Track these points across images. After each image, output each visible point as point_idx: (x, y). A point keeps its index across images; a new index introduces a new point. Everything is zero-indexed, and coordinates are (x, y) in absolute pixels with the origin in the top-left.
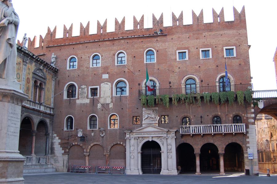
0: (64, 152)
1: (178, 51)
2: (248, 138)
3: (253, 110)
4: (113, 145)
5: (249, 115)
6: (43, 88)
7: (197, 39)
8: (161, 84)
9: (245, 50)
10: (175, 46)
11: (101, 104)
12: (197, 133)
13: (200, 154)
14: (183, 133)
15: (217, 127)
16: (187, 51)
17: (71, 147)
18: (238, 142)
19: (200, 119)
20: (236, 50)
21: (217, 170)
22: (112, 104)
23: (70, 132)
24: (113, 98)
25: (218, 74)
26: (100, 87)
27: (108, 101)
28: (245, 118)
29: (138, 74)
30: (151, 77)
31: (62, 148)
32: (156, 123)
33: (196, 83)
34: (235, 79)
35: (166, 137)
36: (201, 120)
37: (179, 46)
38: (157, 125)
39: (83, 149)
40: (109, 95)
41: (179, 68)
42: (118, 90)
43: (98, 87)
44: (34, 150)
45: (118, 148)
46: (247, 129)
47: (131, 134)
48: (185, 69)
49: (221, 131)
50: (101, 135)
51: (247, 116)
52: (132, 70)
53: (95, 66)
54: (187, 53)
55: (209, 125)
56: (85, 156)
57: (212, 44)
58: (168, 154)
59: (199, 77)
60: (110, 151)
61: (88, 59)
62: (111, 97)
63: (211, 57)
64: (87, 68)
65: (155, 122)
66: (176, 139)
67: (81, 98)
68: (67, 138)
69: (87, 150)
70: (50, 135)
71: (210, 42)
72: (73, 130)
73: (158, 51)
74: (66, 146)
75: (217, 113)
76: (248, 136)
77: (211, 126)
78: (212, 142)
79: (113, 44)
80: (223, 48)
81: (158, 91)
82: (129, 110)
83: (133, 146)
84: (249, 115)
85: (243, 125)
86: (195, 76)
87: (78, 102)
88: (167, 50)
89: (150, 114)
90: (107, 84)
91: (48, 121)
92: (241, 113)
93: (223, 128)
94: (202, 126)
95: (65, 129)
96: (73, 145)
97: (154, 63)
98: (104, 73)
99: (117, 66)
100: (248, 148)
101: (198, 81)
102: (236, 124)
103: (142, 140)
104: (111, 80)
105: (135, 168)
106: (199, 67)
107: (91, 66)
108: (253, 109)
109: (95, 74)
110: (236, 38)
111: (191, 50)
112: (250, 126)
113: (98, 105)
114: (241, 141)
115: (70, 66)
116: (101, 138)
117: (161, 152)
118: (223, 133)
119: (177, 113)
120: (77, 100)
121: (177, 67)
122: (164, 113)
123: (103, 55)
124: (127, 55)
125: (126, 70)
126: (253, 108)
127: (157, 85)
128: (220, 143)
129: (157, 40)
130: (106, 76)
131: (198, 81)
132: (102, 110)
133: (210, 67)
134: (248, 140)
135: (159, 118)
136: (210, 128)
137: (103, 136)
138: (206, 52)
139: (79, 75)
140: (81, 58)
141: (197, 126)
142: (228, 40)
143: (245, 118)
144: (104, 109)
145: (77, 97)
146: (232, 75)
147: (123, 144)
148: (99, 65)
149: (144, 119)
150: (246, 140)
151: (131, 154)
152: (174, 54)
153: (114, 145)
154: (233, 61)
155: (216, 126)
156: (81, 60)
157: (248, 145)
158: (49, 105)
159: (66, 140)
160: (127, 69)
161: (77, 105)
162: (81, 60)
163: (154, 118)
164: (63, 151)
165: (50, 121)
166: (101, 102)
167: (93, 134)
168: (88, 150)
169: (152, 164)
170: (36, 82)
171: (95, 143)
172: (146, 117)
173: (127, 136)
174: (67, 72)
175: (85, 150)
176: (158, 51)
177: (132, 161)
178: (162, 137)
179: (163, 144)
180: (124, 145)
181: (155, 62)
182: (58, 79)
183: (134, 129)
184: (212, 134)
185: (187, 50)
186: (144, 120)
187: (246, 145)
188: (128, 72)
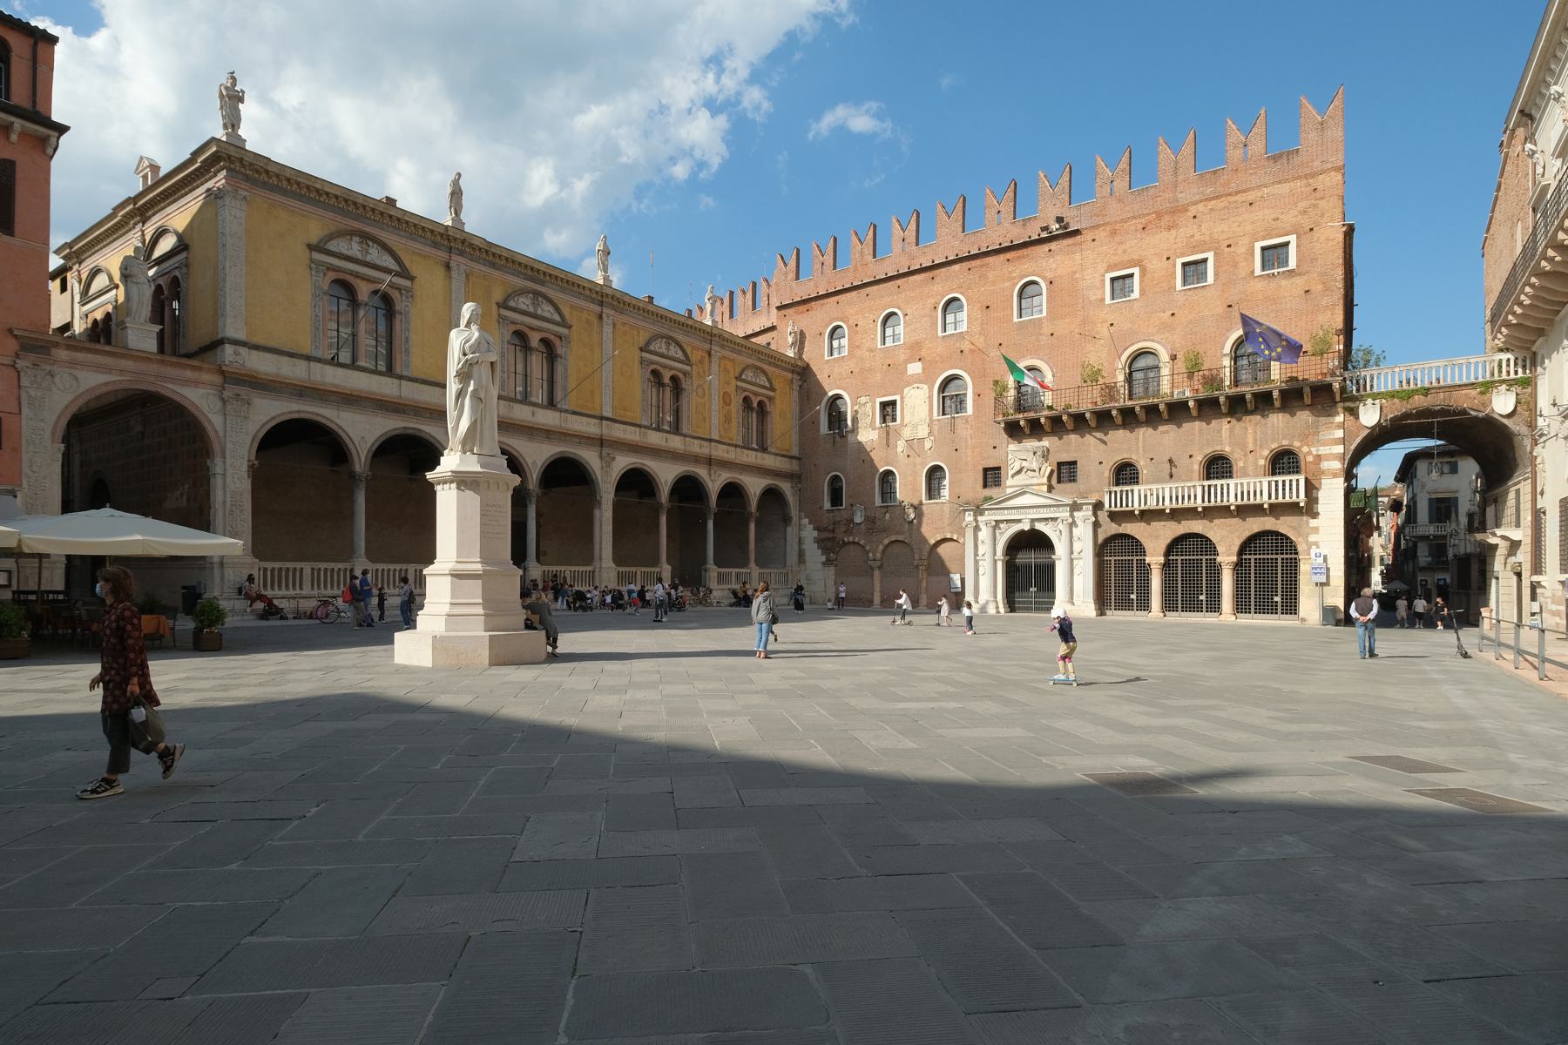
1: (1109, 276)
3: (1339, 434)
21: (1214, 606)
25: (1230, 330)
28: (1310, 459)
37: (1114, 260)
38: (1045, 488)
43: (897, 398)
54: (1136, 278)
64: (871, 351)
70: (795, 519)
74: (830, 544)
91: (786, 487)
92: (1297, 444)
93: (1232, 491)
94: (1167, 487)
95: (827, 505)
101: (1164, 356)
104: (926, 378)
110: (1303, 205)
125: (966, 346)
126: (1342, 426)
130: (915, 368)
131: (1164, 356)
141: (1154, 487)
143: (1310, 459)
154: (1284, 283)
168: (879, 555)
170: (746, 399)
171: (893, 538)
172: (1017, 468)
181: (1045, 313)
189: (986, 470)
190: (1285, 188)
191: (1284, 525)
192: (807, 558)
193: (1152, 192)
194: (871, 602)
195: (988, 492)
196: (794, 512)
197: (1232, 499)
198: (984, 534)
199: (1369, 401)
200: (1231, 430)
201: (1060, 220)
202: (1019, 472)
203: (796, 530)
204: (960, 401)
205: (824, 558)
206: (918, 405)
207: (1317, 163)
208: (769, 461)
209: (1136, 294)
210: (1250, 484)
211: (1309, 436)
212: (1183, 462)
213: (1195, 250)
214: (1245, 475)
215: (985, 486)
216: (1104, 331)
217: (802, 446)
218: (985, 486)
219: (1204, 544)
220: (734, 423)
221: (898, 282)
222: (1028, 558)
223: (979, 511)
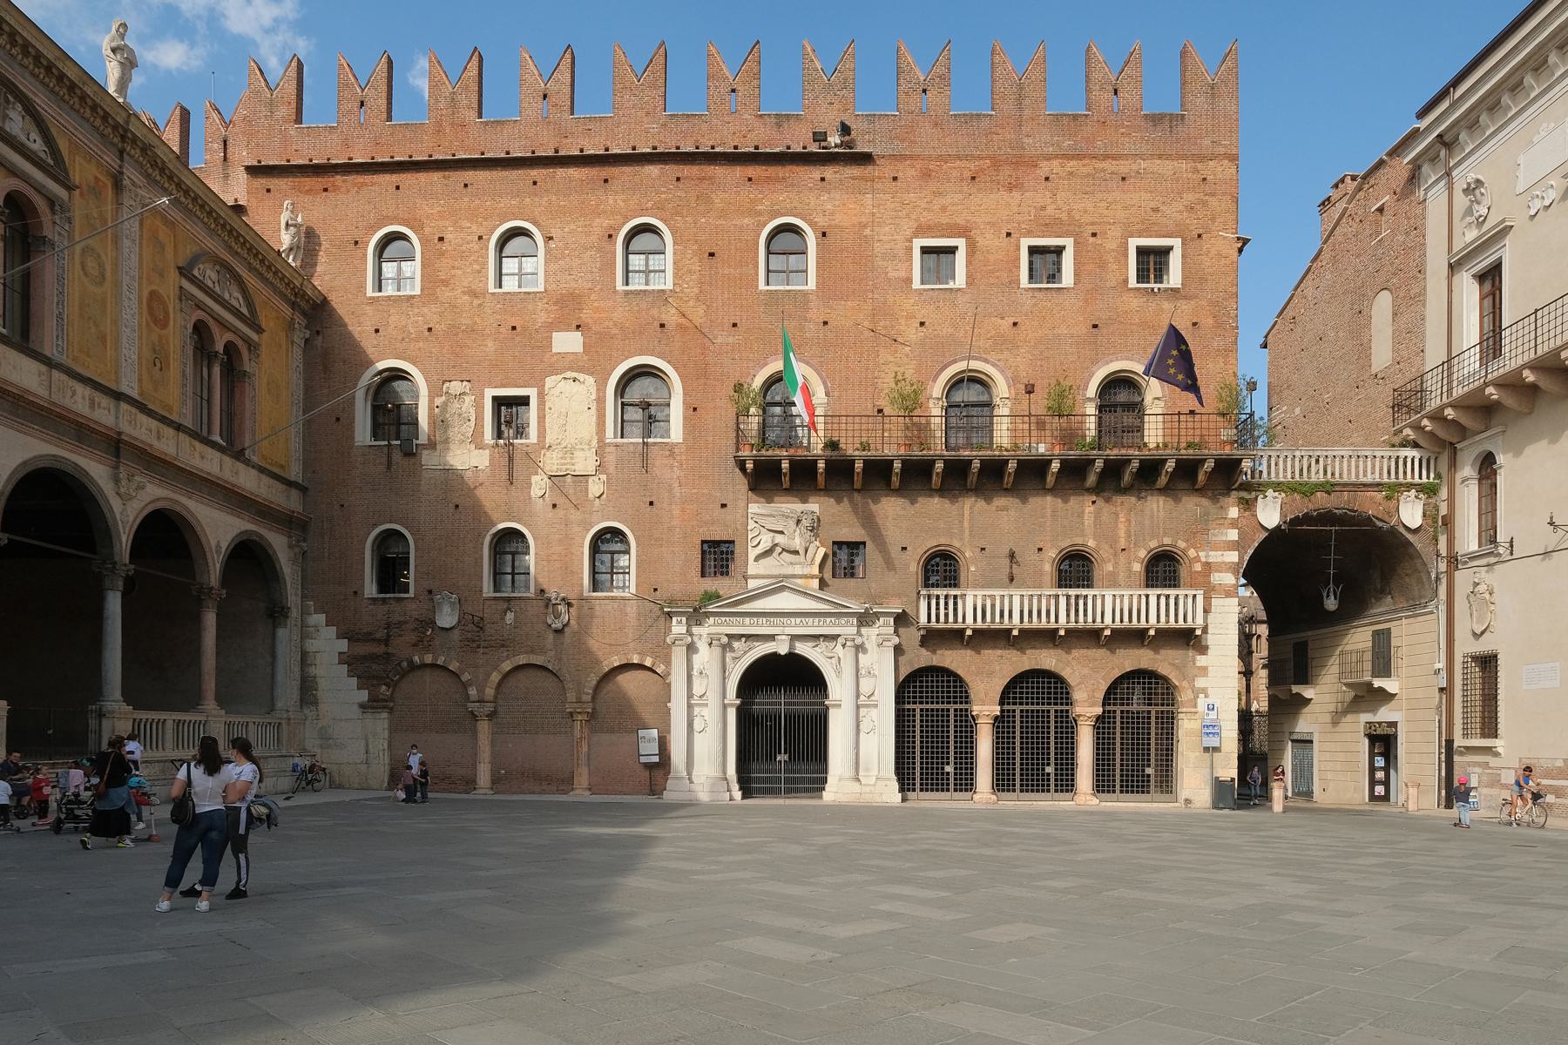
1: (919, 243)
2: (1203, 650)
3: (1233, 535)
5: (1215, 557)
11: (550, 477)
13: (996, 718)
17: (404, 674)
18: (1163, 669)
19: (1007, 561)
22: (603, 477)
25: (1095, 362)
27: (585, 462)
28: (1198, 567)
29: (730, 339)
32: (812, 577)
33: (997, 401)
37: (926, 217)
38: (816, 582)
39: (465, 686)
41: (922, 324)
42: (634, 414)
43: (532, 392)
44: (210, 685)
48: (947, 331)
54: (961, 257)
56: (474, 716)
60: (594, 698)
62: (594, 443)
64: (473, 294)
65: (807, 571)
68: (381, 634)
69: (481, 691)
70: (295, 613)
71: (1069, 212)
73: (824, 234)
74: (380, 668)
75: (1079, 541)
82: (683, 510)
86: (994, 365)
88: (867, 232)
92: (1181, 544)
95: (370, 589)
96: (413, 667)
97: (805, 294)
99: (627, 293)
101: (1002, 389)
102: (1166, 591)
104: (591, 363)
106: (1015, 324)
107: (492, 289)
109: (514, 328)
110: (1189, 197)
111: (981, 241)
113: (535, 479)
116: (551, 636)
120: (425, 452)
121: (910, 317)
125: (671, 317)
128: (1086, 671)
129: (823, 179)
130: (568, 342)
132: (554, 506)
133: (1063, 330)
135: (822, 551)
137: (558, 625)
139: (430, 330)
142: (1152, 204)
144: (560, 501)
150: (1194, 661)
152: (901, 253)
156: (442, 254)
157: (1200, 683)
162: (442, 254)
163: (802, 552)
166: (547, 469)
168: (490, 692)
171: (522, 659)
175: (473, 692)
176: (824, 234)
178: (834, 637)
179: (839, 673)
181: (812, 284)
182: (319, 341)
186: (757, 559)
190: (1166, 167)
191: (1163, 662)
193: (985, 123)
194: (470, 783)
196: (293, 598)
198: (705, 657)
199: (1270, 492)
200: (1097, 515)
201: (845, 130)
202: (768, 553)
203: (296, 637)
204: (651, 417)
205: (364, 696)
206: (572, 416)
207: (1207, 142)
209: (960, 280)
210: (1115, 601)
211: (1199, 533)
212: (1027, 556)
213: (1050, 227)
214: (1114, 584)
216: (912, 334)
219: (1051, 686)
221: (535, 173)
222: (779, 703)
223: (697, 616)
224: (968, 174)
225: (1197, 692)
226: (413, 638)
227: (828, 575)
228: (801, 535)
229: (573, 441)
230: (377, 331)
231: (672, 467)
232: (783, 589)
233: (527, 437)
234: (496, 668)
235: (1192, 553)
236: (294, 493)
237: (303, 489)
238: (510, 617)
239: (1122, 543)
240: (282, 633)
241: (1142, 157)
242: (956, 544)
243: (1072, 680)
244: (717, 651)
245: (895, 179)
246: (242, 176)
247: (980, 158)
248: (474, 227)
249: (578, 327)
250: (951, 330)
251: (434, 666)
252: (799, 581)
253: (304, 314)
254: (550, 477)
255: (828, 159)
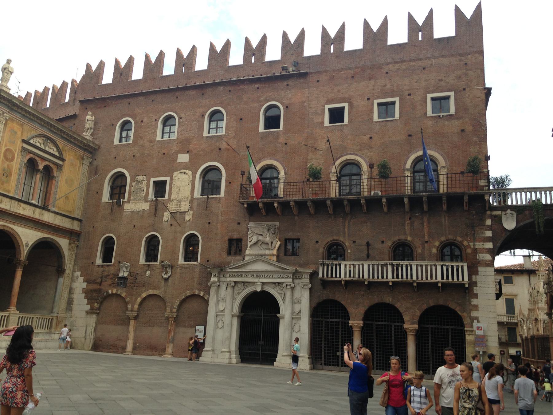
0: (90, 309)
1: (327, 107)
2: (477, 298)
3: (489, 234)
4: (184, 297)
5: (479, 245)
6: (53, 177)
7: (370, 79)
8: (289, 173)
9: (477, 100)
10: (323, 96)
11: (171, 213)
12: (354, 279)
14: (325, 278)
15: (400, 268)
16: (346, 105)
18: (452, 305)
19: (366, 247)
20: (456, 100)
22: (191, 212)
23: (106, 269)
24: (195, 201)
25: (410, 152)
26: (171, 180)
27: (185, 206)
30: (271, 159)
31: (88, 299)
33: (362, 172)
34: (448, 162)
35: (290, 285)
36: (368, 250)
38: (275, 258)
39: (127, 304)
40: (187, 196)
42: (206, 184)
43: (168, 179)
45: (194, 305)
46: (474, 277)
47: (222, 276)
49: (409, 277)
50: (163, 275)
51: (474, 245)
52: (234, 147)
53: (166, 137)
55: (382, 263)
57: (401, 88)
58: (294, 321)
59: (367, 160)
61: (153, 123)
62: (189, 198)
63: (397, 116)
64: (151, 141)
65: (271, 252)
66: (310, 289)
67: (135, 199)
68: (99, 280)
69: (133, 306)
70: (67, 271)
72: (112, 263)
73: (287, 107)
75: (403, 237)
76: (475, 292)
77: (386, 265)
78: (388, 299)
79: (203, 94)
80: (426, 97)
81: (282, 187)
83: (224, 300)
84: (479, 245)
85: (462, 267)
87: (128, 207)
88: (305, 104)
89: (261, 235)
90: (185, 173)
91: (63, 243)
92: (459, 239)
93: (416, 271)
98: (182, 152)
99: (207, 137)
100: (475, 321)
101: (365, 167)
103: (243, 288)
104: (192, 166)
105: (223, 350)
106: (371, 138)
107: (159, 138)
108: (488, 230)
109: (164, 154)
110: (458, 73)
111: (355, 103)
112: (481, 269)
113: (165, 213)
114: (458, 303)
115: (121, 138)
116: (163, 282)
117: (278, 315)
118: (414, 281)
119: (315, 236)
122: (290, 233)
123: (183, 116)
124: (227, 116)
125: (223, 145)
127: (280, 177)
130: (183, 158)
131: (365, 167)
132: (171, 225)
134: (474, 302)
135: (279, 243)
136: (385, 268)
137: (166, 277)
138: (386, 108)
140: (142, 121)
141: (356, 263)
142: (440, 78)
143: (469, 251)
144: (174, 223)
145: (126, 199)
146: (442, 155)
147: (204, 295)
148: (174, 136)
149: (249, 244)
150: (470, 302)
151: (218, 319)
153: (187, 298)
154: (446, 123)
155: (398, 266)
157: (474, 314)
158: (70, 212)
159: (96, 283)
160: (224, 143)
161: (125, 214)
163: (270, 244)
164: (89, 306)
165: (70, 244)
166: (170, 209)
167: (148, 273)
168: (136, 307)
169: (261, 343)
171: (151, 292)
172: (254, 239)
173: (214, 279)
174: (114, 149)
175: (129, 306)
176: (287, 107)
177: (220, 334)
179: (284, 300)
180: (206, 298)
182: (95, 163)
183: (229, 263)
184: (388, 282)
185: (348, 103)
186: (250, 247)
187: (470, 312)
188: (227, 150)
189: (231, 241)
190: (447, 61)
192: (75, 306)
195: (230, 258)
197: (414, 278)
199: (509, 211)
200: (412, 224)
202: (255, 244)
205: (88, 307)
206: (184, 187)
208: (47, 217)
214: (423, 259)
215: (229, 253)
216: (324, 145)
217: (85, 210)
218: (229, 253)
220: (14, 178)
224: (350, 76)
225: (473, 319)
226: (109, 282)
227: (282, 254)
228: (269, 236)
229: (181, 198)
230: (115, 158)
231: (219, 207)
232: (258, 260)
233: (164, 197)
234: (140, 295)
235: (465, 243)
236: (76, 222)
237: (80, 221)
238: (148, 273)
239: (426, 238)
240: (61, 280)
241: (434, 58)
242: (342, 239)
243: (401, 310)
244: (230, 289)
245: (318, 81)
246: (78, 103)
247: (356, 68)
248: (154, 116)
249: (188, 152)
250: (341, 143)
251: (117, 295)
252: (267, 257)
253: (91, 153)
254: (171, 213)
255: (289, 77)
